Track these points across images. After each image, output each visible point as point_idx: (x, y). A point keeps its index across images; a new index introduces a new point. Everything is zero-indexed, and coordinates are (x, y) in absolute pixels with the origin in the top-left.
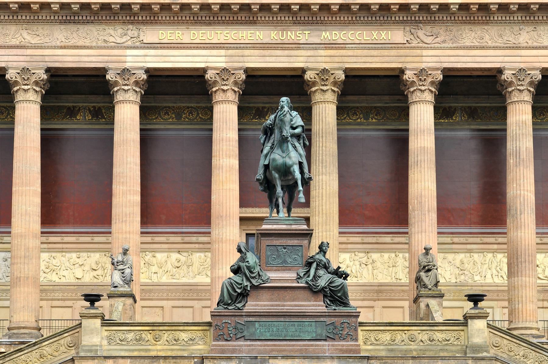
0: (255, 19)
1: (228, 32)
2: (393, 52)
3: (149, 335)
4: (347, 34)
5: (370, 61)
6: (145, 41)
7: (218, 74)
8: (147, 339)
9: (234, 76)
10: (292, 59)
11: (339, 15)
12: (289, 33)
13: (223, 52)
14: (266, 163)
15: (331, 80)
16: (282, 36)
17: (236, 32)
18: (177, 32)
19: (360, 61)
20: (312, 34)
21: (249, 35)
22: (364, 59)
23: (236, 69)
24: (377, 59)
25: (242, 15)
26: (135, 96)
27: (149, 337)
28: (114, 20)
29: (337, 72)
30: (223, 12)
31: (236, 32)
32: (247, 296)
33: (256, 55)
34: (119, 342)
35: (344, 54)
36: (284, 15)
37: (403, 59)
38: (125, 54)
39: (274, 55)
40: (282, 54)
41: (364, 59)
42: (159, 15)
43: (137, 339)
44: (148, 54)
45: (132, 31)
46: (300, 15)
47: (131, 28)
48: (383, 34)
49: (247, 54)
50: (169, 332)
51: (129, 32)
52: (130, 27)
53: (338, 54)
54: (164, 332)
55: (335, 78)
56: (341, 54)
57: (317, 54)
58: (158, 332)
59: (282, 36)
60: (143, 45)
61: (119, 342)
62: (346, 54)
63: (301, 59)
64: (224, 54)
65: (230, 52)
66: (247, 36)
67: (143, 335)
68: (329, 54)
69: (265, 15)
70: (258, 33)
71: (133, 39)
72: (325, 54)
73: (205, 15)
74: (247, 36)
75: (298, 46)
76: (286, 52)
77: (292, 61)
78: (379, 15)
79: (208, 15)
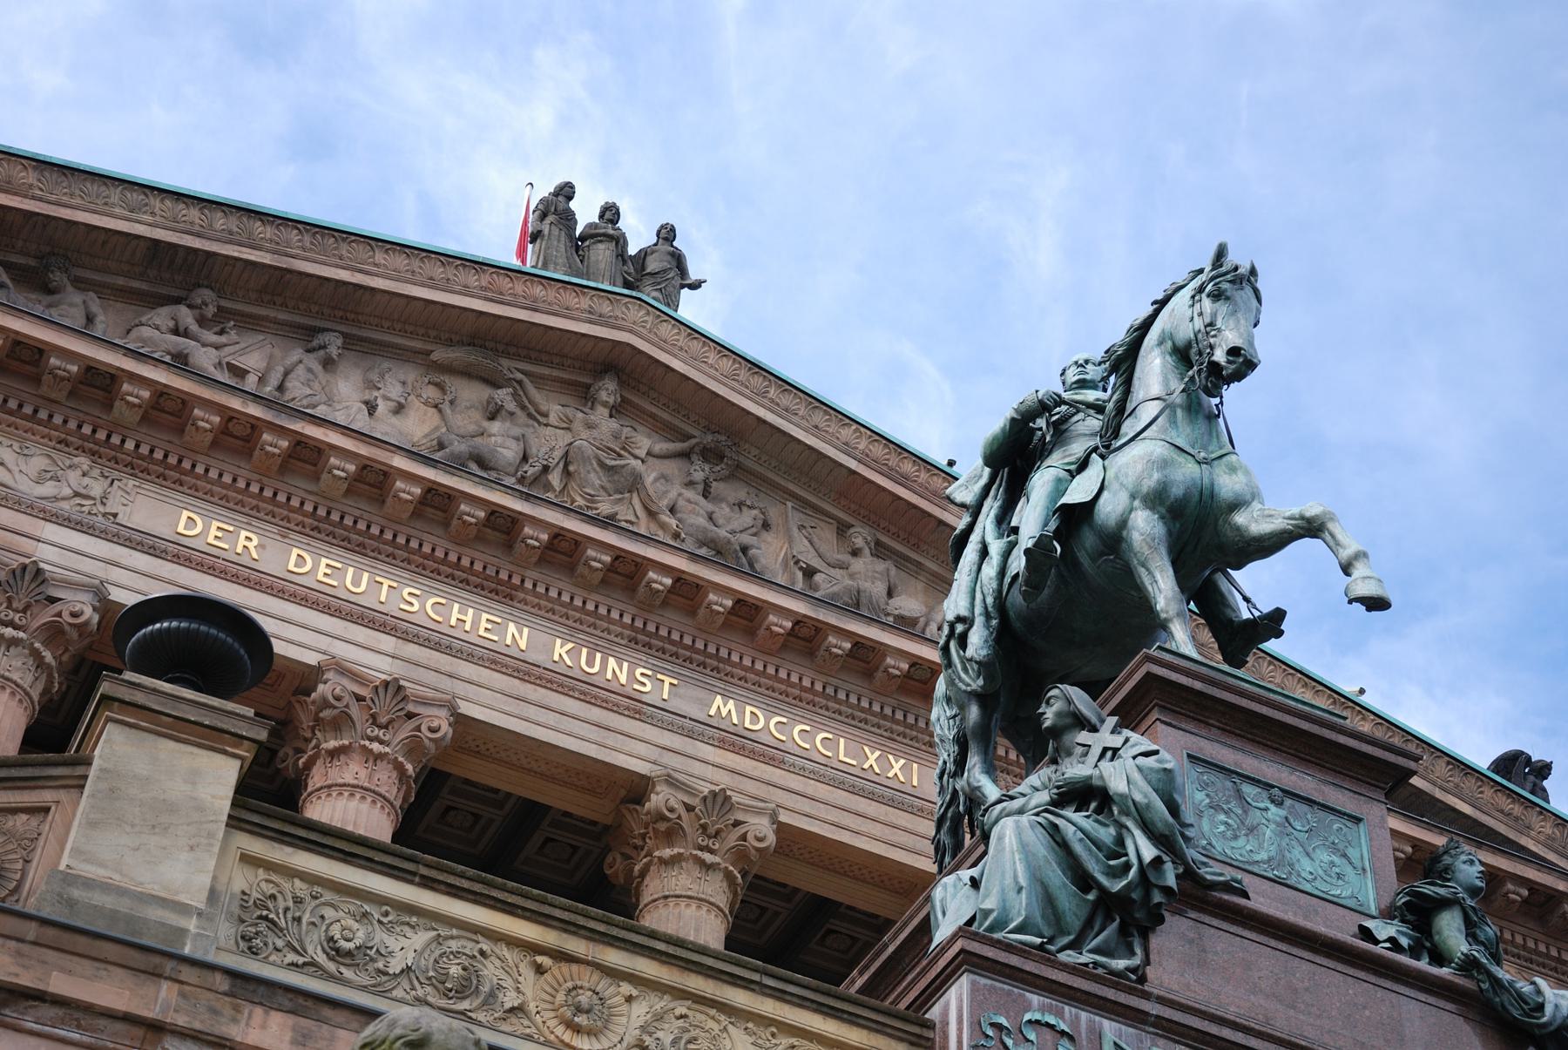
0: (516, 580)
1: (418, 592)
3: (528, 974)
4: (787, 728)
5: (853, 826)
6: (120, 519)
7: (360, 699)
8: (511, 1000)
9: (412, 724)
10: (611, 739)
11: (777, 661)
12: (612, 662)
13: (387, 642)
14: (1079, 492)
15: (732, 839)
16: (590, 663)
17: (443, 601)
18: (244, 534)
19: (823, 815)
20: (681, 691)
21: (484, 624)
22: (834, 815)
23: (425, 702)
24: (877, 830)
25: (477, 555)
26: (30, 678)
27: (528, 988)
28: (33, 418)
29: (752, 820)
30: (418, 525)
31: (443, 601)
32: (1145, 934)
33: (497, 686)
34: (321, 958)
35: (775, 780)
36: (610, 602)
38: (38, 534)
39: (554, 706)
40: (582, 715)
41: (834, 815)
42: (200, 458)
43: (444, 977)
44: (124, 562)
45: (81, 477)
46: (658, 619)
47: (85, 467)
48: (897, 765)
49: (466, 675)
50: (661, 1003)
51: (73, 477)
52: (84, 461)
53: (755, 774)
54: (627, 988)
55: (744, 838)
56: (766, 777)
57: (690, 751)
58: (588, 977)
59: (590, 663)
60: (114, 528)
61: (321, 958)
62: (781, 782)
63: (641, 749)
64: (390, 650)
65: (412, 650)
66: (476, 623)
67: (491, 971)
68: (729, 764)
69: (548, 580)
70: (512, 628)
71: (78, 500)
72: (718, 760)
73: (357, 513)
74: (476, 623)
75: (636, 707)
76: (596, 714)
77: (610, 742)
78: (894, 703)
79: (366, 516)
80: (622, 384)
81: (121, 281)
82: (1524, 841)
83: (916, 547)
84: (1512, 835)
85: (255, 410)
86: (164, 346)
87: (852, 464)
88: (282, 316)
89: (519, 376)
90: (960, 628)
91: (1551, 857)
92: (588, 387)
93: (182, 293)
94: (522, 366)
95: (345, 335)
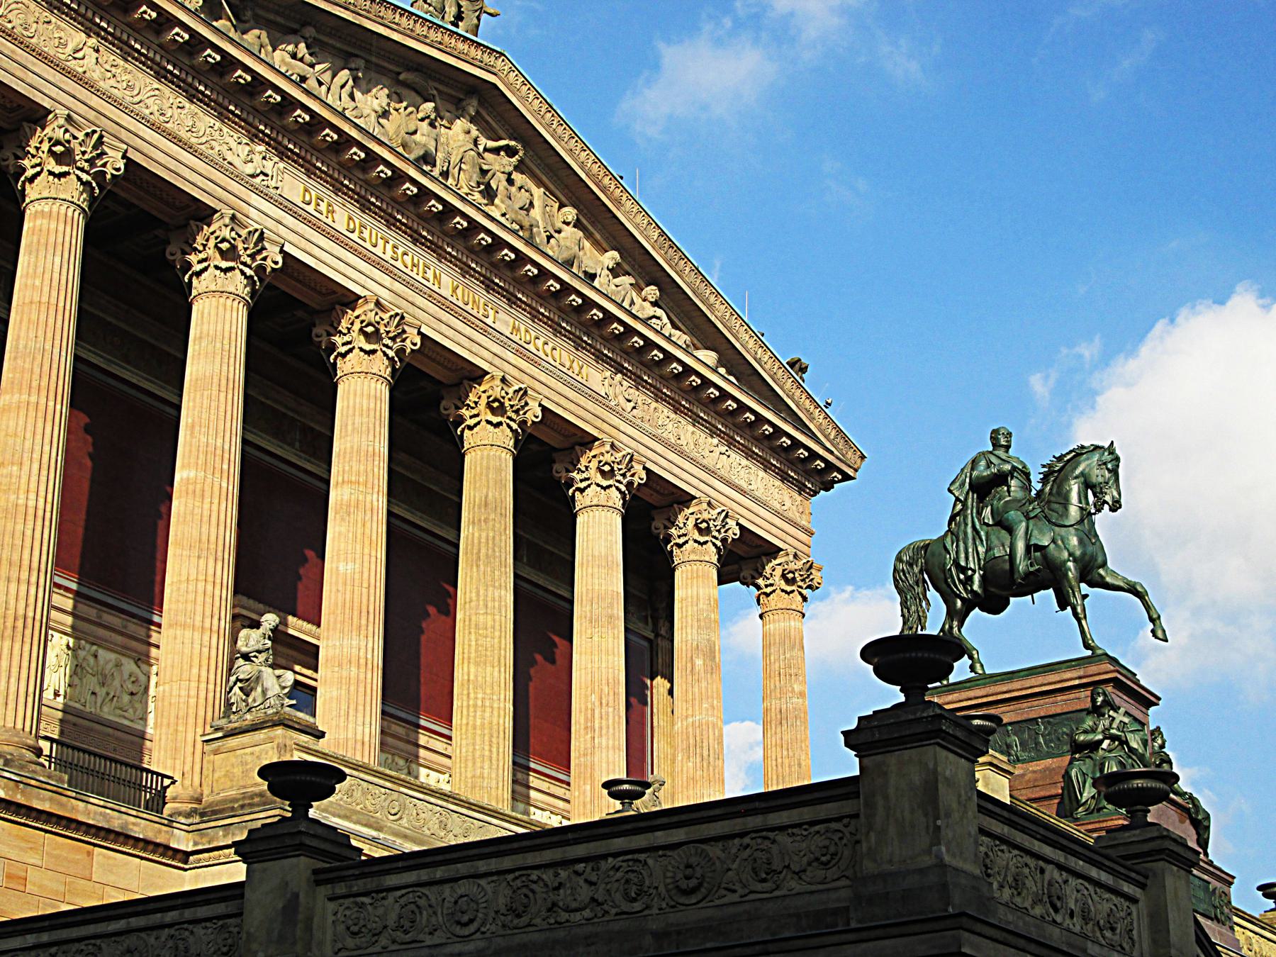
2: (590, 405)
10: (476, 348)
33: (431, 311)
37: (599, 423)
76: (468, 331)
80: (480, 103)
81: (272, 17)
82: (812, 426)
83: (593, 224)
84: (807, 422)
85: (354, 133)
86: (297, 71)
87: (583, 176)
88: (338, 45)
89: (435, 92)
90: (970, 573)
91: (819, 435)
92: (461, 100)
93: (296, 26)
94: (441, 87)
95: (367, 61)
